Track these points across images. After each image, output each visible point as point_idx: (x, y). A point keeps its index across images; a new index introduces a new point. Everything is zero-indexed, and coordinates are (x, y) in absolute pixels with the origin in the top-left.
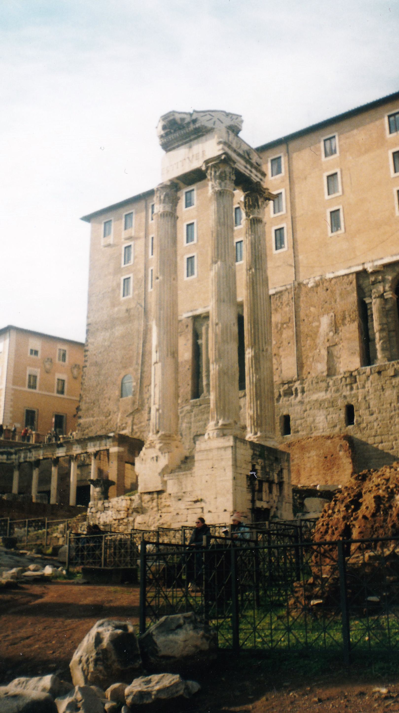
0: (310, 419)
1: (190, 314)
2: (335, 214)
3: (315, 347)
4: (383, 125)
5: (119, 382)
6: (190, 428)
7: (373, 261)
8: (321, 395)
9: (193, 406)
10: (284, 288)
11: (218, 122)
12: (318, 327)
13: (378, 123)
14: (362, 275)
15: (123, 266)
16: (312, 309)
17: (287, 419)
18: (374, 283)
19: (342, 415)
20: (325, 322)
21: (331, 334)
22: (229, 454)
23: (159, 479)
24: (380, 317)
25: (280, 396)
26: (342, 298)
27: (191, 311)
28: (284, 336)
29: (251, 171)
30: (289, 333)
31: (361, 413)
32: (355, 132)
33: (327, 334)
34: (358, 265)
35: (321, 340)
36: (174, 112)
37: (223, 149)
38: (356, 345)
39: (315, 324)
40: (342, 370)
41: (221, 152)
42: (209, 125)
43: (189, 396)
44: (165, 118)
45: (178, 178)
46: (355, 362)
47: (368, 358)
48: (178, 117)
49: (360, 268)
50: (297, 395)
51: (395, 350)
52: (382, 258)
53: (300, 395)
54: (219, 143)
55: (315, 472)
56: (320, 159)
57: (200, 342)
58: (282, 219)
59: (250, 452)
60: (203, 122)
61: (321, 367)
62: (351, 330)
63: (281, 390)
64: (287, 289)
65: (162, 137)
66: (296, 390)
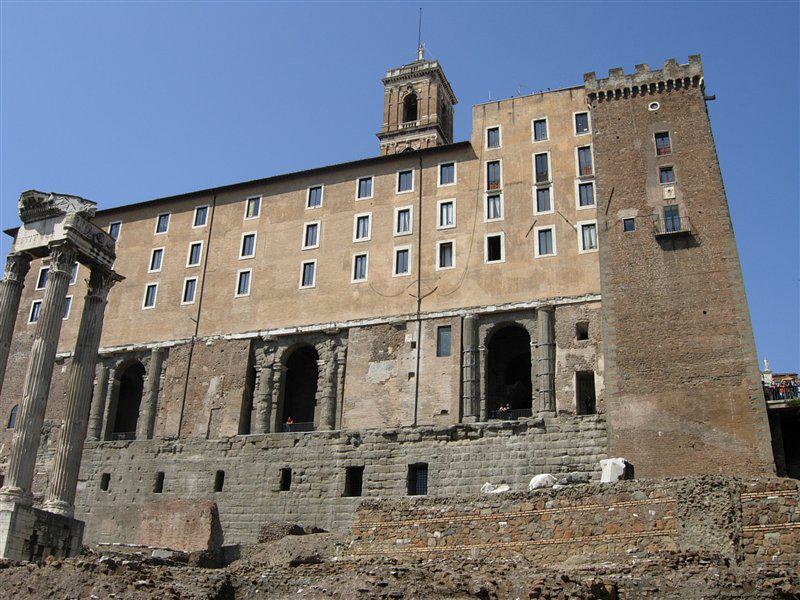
0: (182, 480)
3: (200, 406)
4: (305, 195)
5: (9, 412)
8: (196, 458)
10: (183, 342)
11: (71, 207)
12: (207, 387)
13: (300, 192)
14: (256, 342)
15: (36, 289)
16: (205, 368)
17: (161, 476)
18: (267, 352)
19: (212, 480)
20: (215, 382)
22: (8, 518)
25: (159, 452)
26: (234, 363)
28: (174, 391)
29: (98, 254)
30: (179, 389)
31: (230, 482)
32: (278, 197)
34: (255, 332)
35: (207, 401)
36: (34, 191)
37: (67, 234)
38: (237, 412)
39: (204, 384)
40: (220, 435)
41: (65, 237)
42: (62, 208)
44: (25, 194)
45: (29, 250)
46: (230, 428)
47: (245, 427)
48: (36, 196)
49: (256, 335)
54: (65, 228)
55: (176, 534)
56: (242, 218)
58: (195, 271)
59: (35, 518)
61: (202, 428)
62: (237, 395)
64: (186, 343)
65: (22, 210)
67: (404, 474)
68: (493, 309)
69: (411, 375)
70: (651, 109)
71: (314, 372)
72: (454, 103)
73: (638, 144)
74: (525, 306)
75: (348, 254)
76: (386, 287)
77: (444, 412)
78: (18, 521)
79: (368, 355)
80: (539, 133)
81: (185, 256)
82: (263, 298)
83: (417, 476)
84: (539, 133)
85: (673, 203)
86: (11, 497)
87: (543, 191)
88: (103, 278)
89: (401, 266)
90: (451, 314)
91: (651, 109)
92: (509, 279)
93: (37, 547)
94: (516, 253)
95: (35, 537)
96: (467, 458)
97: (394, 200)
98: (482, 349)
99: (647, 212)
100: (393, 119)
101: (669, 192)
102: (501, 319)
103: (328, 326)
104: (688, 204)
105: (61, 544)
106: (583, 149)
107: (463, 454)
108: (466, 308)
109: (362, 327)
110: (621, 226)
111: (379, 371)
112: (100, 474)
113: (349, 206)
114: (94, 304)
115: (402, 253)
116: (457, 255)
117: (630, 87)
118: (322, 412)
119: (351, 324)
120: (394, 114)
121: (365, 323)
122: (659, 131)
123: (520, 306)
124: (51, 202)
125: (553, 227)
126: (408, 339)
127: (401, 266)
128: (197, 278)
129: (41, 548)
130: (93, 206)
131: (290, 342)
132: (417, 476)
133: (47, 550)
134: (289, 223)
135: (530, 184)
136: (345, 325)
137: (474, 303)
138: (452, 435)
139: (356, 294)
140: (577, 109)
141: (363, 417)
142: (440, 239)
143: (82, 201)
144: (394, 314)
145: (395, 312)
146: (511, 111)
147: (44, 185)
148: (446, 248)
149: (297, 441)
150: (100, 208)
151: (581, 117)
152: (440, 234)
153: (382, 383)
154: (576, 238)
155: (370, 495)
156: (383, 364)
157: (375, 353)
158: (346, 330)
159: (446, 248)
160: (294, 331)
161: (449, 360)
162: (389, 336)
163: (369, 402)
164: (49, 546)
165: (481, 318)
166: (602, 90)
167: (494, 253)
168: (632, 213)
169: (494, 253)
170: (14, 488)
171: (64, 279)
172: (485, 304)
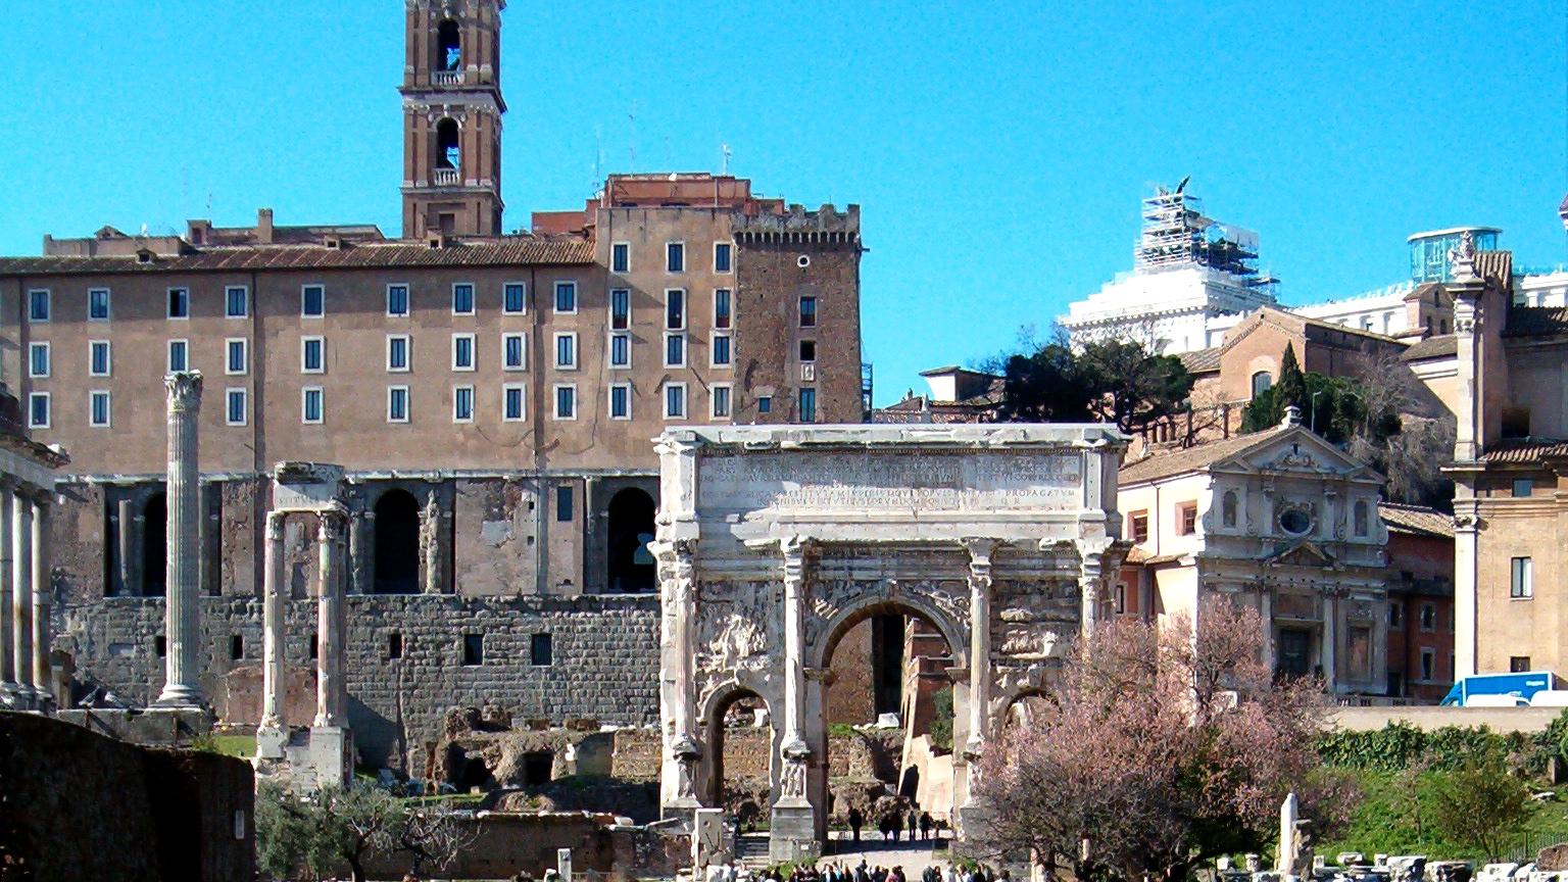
1: (102, 480)
2: (312, 395)
6: (104, 634)
7: (356, 473)
9: (108, 606)
21: (299, 549)
23: (279, 750)
24: (358, 542)
27: (104, 476)
33: (295, 549)
43: (101, 591)
50: (251, 614)
51: (371, 581)
52: (367, 473)
53: (255, 615)
57: (113, 519)
60: (320, 474)
63: (233, 605)
66: (252, 608)
67: (528, 644)
68: (618, 474)
69: (531, 539)
70: (800, 265)
71: (415, 524)
72: (501, 8)
73: (782, 306)
74: (652, 474)
75: (448, 386)
76: (496, 432)
77: (567, 582)
79: (482, 513)
80: (675, 265)
81: (222, 358)
82: (340, 429)
83: (541, 648)
84: (675, 265)
85: (811, 386)
87: (675, 342)
89: (513, 412)
90: (572, 474)
91: (800, 265)
92: (635, 441)
94: (642, 411)
96: (594, 630)
97: (502, 322)
98: (606, 514)
99: (783, 392)
100: (423, 64)
101: (807, 372)
102: (625, 485)
103: (431, 475)
104: (825, 388)
106: (723, 294)
107: (588, 627)
108: (590, 470)
109: (471, 480)
110: (757, 405)
111: (492, 531)
112: (151, 637)
113: (445, 323)
115: (513, 395)
116: (578, 404)
117: (782, 232)
118: (429, 573)
119: (458, 475)
120: (423, 51)
121: (475, 475)
122: (806, 295)
123: (646, 474)
124: (313, 473)
125: (683, 385)
126: (524, 496)
127: (513, 412)
128: (244, 390)
131: (385, 488)
132: (541, 648)
134: (366, 332)
135: (661, 330)
136: (451, 476)
137: (596, 464)
138: (574, 607)
139: (460, 437)
140: (718, 238)
141: (479, 582)
142: (562, 382)
144: (506, 467)
145: (507, 464)
146: (642, 224)
148: (565, 395)
149: (404, 605)
151: (723, 250)
152: (558, 376)
153: (498, 546)
154: (708, 401)
155: (492, 664)
156: (499, 524)
157: (489, 510)
158: (455, 479)
159: (565, 395)
160: (389, 476)
161: (571, 525)
162: (500, 497)
163: (485, 567)
165: (602, 484)
166: (750, 229)
167: (619, 410)
168: (768, 392)
169: (619, 410)
172: (610, 466)
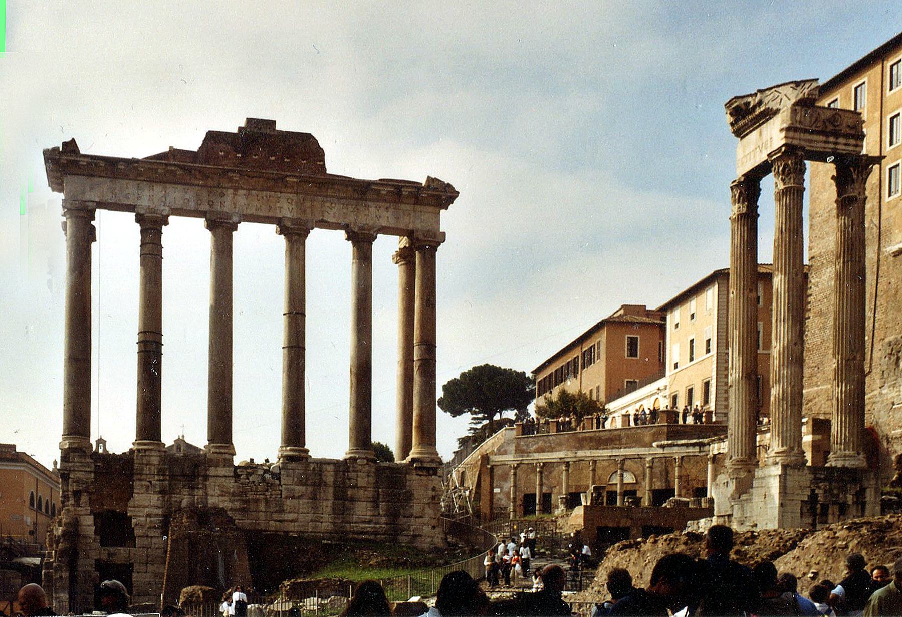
78: (789, 484)
86: (778, 459)
88: (853, 172)
93: (819, 506)
95: (813, 497)
105: (850, 498)
114: (850, 200)
129: (825, 507)
130: (814, 85)
133: (833, 509)
143: (797, 84)
147: (745, 87)
150: (821, 82)
164: (834, 503)
170: (781, 449)
171: (793, 196)
